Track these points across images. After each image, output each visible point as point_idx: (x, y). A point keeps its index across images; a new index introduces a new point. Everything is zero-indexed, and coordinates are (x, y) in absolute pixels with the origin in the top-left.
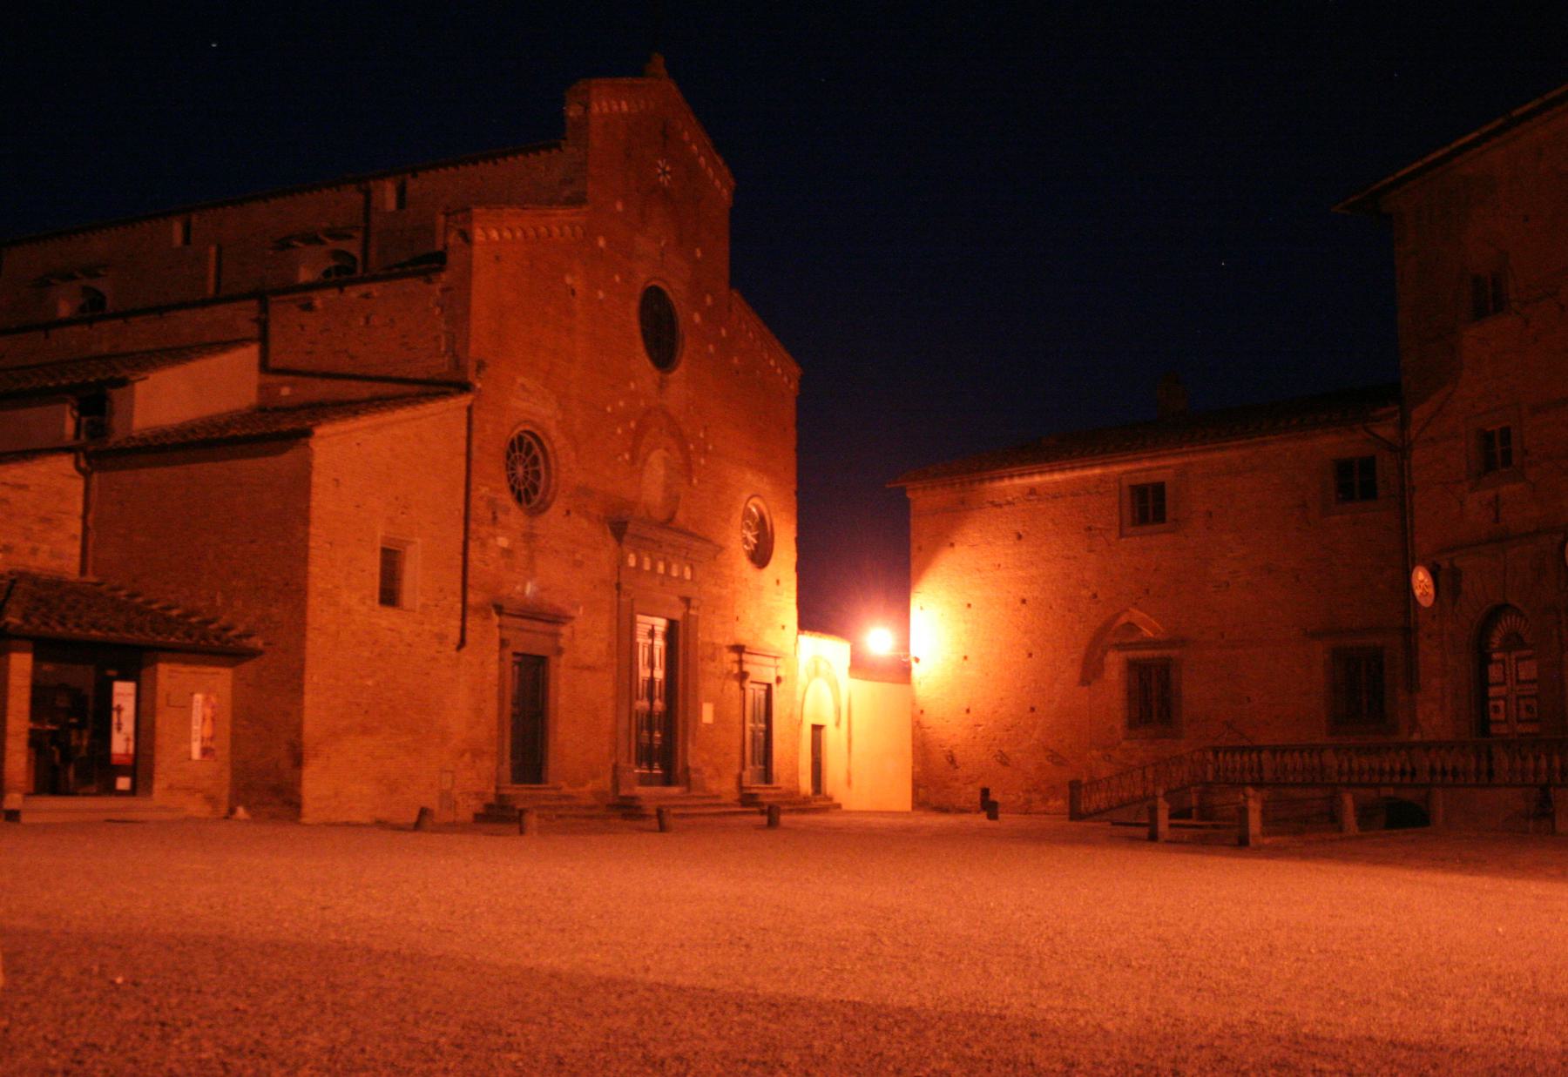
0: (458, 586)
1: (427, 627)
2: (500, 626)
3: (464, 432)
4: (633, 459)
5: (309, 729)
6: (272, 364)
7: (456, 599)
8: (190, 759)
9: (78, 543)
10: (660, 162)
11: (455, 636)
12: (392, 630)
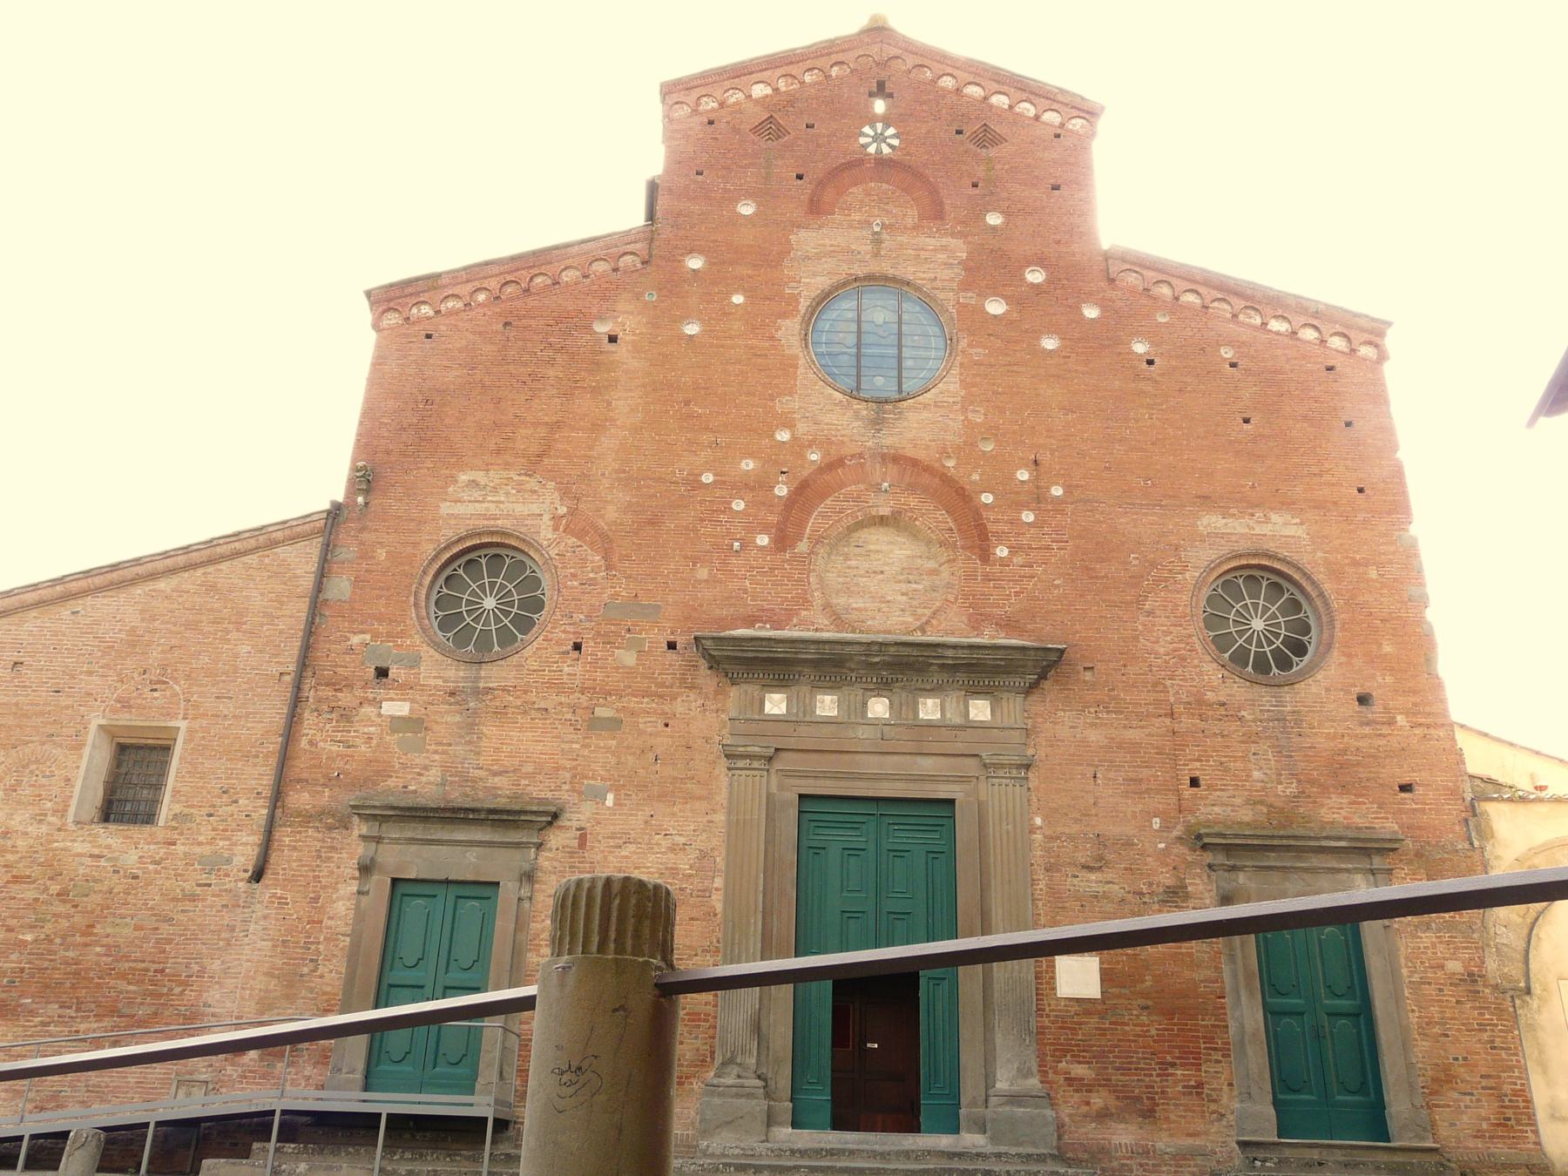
1: (180, 848)
3: (313, 567)
4: (782, 541)
11: (245, 853)
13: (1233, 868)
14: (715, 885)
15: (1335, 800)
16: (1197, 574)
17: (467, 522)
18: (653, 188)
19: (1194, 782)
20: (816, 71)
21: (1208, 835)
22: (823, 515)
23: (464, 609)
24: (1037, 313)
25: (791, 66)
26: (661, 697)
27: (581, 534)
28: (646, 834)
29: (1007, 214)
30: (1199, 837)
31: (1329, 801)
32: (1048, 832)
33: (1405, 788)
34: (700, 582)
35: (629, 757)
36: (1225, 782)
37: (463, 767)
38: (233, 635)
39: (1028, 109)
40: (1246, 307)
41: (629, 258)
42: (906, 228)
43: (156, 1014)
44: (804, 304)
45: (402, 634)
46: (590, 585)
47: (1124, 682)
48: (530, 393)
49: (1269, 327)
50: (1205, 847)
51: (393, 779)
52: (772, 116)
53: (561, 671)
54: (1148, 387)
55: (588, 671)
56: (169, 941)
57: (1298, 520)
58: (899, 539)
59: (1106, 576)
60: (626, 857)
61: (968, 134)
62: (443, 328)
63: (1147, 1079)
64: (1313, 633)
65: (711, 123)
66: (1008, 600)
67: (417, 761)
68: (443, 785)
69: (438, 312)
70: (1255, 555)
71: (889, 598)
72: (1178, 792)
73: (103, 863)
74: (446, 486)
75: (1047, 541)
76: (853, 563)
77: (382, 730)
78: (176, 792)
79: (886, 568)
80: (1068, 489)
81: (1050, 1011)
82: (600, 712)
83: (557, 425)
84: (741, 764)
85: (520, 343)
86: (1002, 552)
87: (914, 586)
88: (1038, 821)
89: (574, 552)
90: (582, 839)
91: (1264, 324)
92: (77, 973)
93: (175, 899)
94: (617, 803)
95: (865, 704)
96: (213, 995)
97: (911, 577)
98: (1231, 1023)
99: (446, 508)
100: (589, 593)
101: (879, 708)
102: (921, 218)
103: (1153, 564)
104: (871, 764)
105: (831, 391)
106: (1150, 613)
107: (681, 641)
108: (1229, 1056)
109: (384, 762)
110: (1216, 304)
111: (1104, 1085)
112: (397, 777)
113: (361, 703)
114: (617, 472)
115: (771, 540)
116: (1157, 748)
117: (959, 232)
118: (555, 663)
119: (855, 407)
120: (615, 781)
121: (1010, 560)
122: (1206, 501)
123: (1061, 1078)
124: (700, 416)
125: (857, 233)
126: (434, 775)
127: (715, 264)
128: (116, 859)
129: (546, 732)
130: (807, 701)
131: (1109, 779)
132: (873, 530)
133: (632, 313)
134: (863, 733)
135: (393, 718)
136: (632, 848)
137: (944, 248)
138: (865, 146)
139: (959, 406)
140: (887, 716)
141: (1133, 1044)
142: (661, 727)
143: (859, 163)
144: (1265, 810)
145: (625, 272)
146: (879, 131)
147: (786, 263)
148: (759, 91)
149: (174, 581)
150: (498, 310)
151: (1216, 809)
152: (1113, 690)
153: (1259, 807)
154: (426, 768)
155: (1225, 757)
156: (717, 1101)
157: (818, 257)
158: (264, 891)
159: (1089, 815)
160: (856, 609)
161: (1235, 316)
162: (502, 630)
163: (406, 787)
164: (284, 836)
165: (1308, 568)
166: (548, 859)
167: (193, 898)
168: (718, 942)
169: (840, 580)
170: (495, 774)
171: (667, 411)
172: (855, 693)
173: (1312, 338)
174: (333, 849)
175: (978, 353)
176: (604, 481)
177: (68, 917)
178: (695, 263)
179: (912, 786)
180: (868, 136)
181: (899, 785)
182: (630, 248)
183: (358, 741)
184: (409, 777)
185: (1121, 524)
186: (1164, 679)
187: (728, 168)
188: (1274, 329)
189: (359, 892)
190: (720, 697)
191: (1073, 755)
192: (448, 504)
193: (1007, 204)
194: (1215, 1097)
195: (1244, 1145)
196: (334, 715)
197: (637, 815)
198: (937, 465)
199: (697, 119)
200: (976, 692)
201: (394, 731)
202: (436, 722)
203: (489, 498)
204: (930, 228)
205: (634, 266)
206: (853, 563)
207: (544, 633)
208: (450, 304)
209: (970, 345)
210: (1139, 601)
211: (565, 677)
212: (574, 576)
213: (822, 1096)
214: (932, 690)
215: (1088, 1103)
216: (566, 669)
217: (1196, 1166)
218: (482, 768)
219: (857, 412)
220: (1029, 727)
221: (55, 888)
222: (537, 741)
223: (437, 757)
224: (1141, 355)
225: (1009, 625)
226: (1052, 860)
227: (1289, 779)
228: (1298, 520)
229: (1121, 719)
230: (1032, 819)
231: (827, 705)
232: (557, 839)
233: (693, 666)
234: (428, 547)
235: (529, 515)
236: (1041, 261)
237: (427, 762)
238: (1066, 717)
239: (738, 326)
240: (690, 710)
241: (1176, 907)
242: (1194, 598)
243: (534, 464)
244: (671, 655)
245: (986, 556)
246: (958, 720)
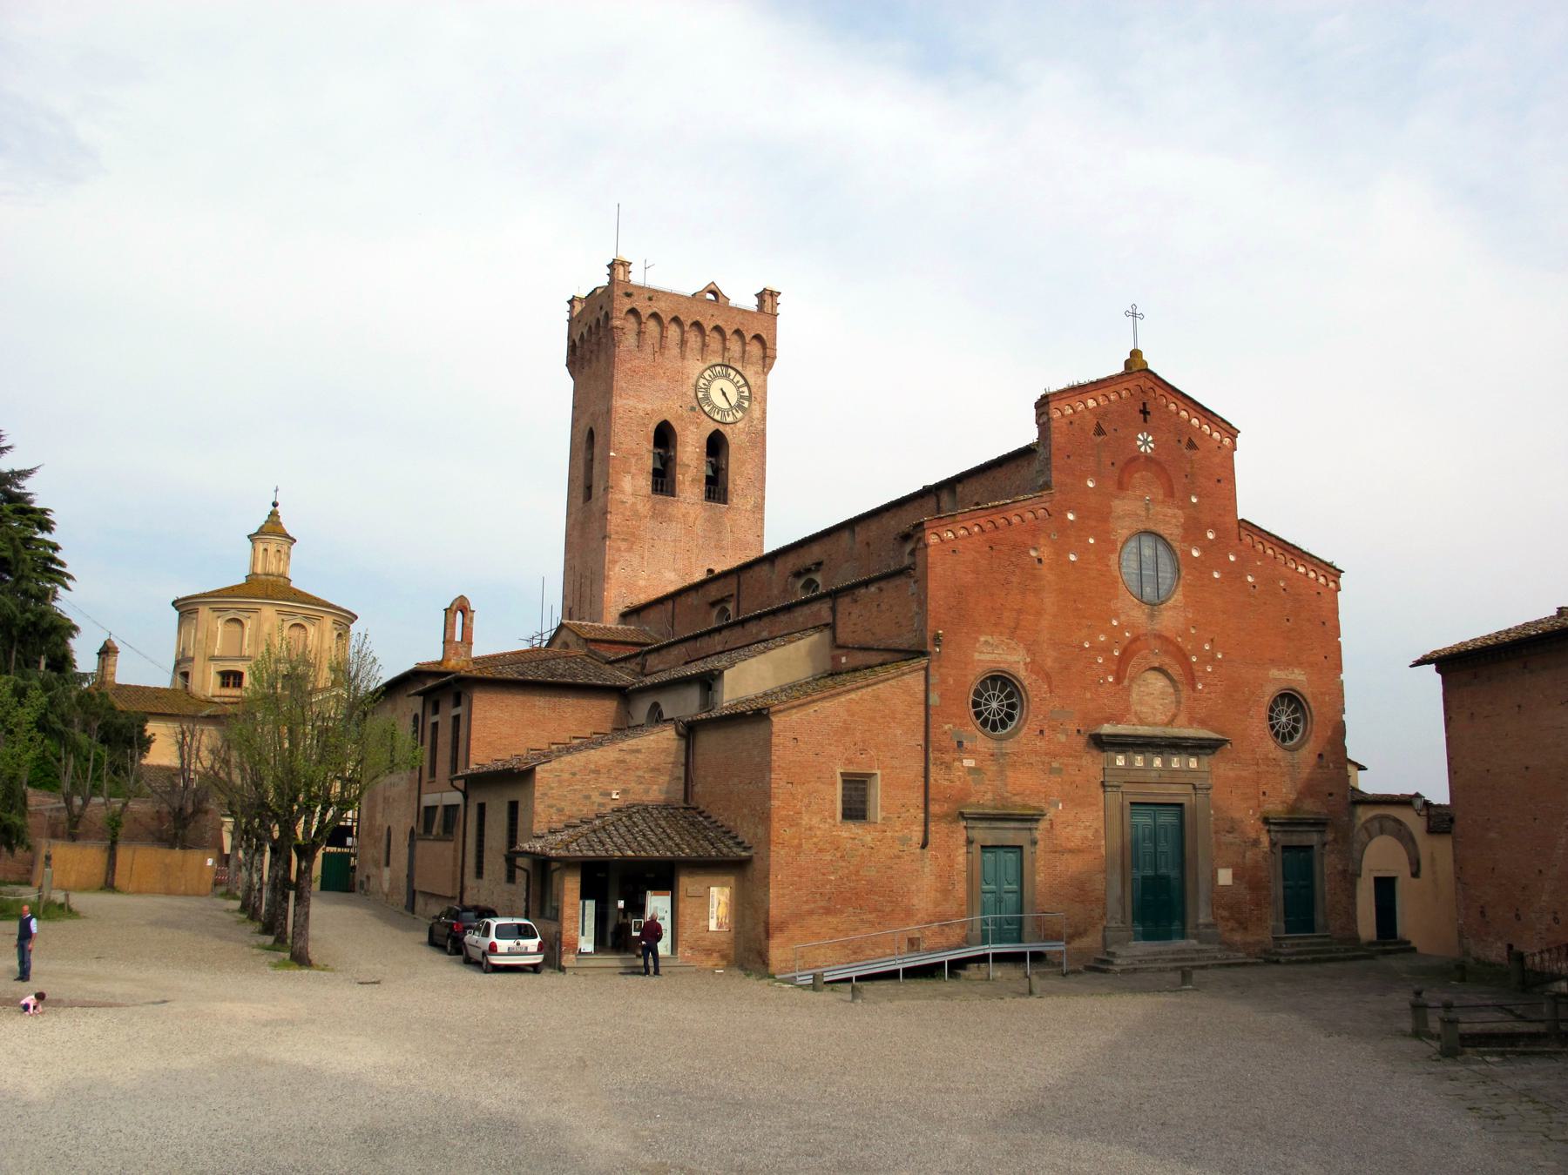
0: (921, 800)
2: (966, 827)
3: (922, 688)
4: (1118, 680)
5: (774, 911)
6: (840, 641)
7: (919, 811)
8: (708, 931)
9: (683, 781)
10: (1140, 436)
11: (917, 836)
12: (854, 839)
19: (1264, 793)
22: (1133, 666)
26: (1076, 757)
27: (1037, 674)
33: (1331, 794)
38: (892, 725)
43: (893, 910)
44: (1119, 545)
56: (892, 877)
62: (961, 547)
65: (1071, 423)
69: (956, 538)
72: (1258, 798)
73: (857, 842)
76: (1142, 689)
78: (882, 806)
82: (1055, 765)
83: (1020, 611)
85: (998, 560)
88: (1212, 812)
90: (1052, 825)
91: (1297, 569)
92: (857, 894)
93: (891, 858)
96: (915, 901)
99: (977, 656)
101: (1157, 762)
102: (1165, 496)
103: (1253, 693)
104: (1156, 789)
105: (1132, 598)
106: (1252, 717)
110: (1279, 556)
114: (1050, 639)
122: (1273, 662)
124: (1081, 609)
126: (989, 796)
128: (861, 840)
133: (1046, 546)
134: (1153, 774)
136: (1070, 828)
138: (1140, 447)
139: (1182, 609)
143: (1135, 459)
145: (1042, 520)
148: (1091, 403)
149: (859, 693)
154: (985, 792)
158: (929, 852)
164: (932, 827)
165: (1306, 696)
167: (899, 857)
170: (1015, 795)
172: (1148, 755)
174: (953, 832)
177: (847, 868)
183: (955, 780)
193: (1199, 490)
195: (1276, 939)
196: (943, 767)
199: (1064, 420)
200: (1192, 755)
206: (1142, 689)
209: (1187, 574)
221: (839, 855)
223: (989, 787)
225: (1203, 723)
231: (1139, 761)
232: (1043, 825)
234: (973, 679)
236: (1214, 527)
238: (1222, 765)
239: (1092, 557)
243: (1013, 632)
245: (1194, 688)
246: (1185, 768)
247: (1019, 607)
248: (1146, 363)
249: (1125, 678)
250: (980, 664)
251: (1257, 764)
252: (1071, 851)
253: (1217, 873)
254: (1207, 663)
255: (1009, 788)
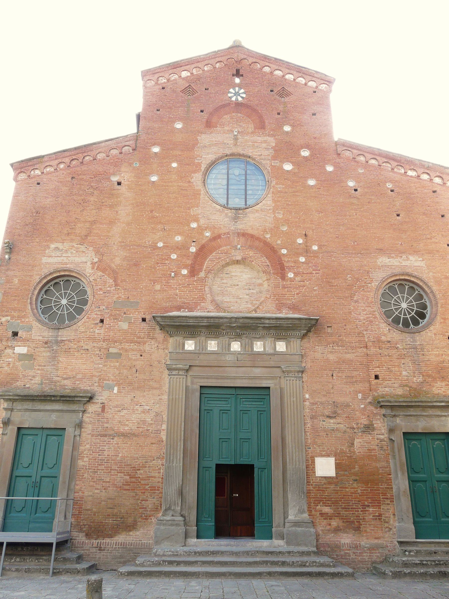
4: (193, 272)
13: (395, 416)
14: (163, 428)
15: (439, 384)
16: (377, 284)
17: (54, 266)
18: (139, 117)
19: (377, 377)
20: (210, 65)
21: (383, 401)
22: (212, 260)
23: (53, 304)
24: (306, 169)
25: (199, 64)
26: (139, 343)
27: (104, 270)
28: (132, 405)
29: (293, 126)
30: (379, 402)
31: (436, 384)
32: (312, 401)
34: (157, 291)
35: (125, 371)
36: (390, 377)
37: (50, 376)
39: (301, 80)
40: (397, 165)
41: (126, 148)
42: (248, 133)
44: (203, 167)
45: (24, 317)
46: (108, 293)
47: (345, 333)
48: (82, 208)
49: (407, 174)
50: (381, 407)
51: (19, 382)
52: (190, 85)
53: (94, 332)
54: (355, 201)
55: (106, 332)
57: (421, 259)
58: (245, 270)
59: (337, 285)
60: (123, 416)
61: (276, 92)
63: (357, 513)
64: (429, 309)
65: (163, 88)
66: (293, 297)
67: (30, 374)
68: (42, 384)
69: (43, 173)
70: (403, 275)
71: (241, 297)
72: (369, 382)
74: (45, 250)
75: (311, 270)
76: (225, 281)
77: (15, 360)
79: (239, 283)
80: (320, 247)
81: (313, 482)
82: (112, 350)
83: (93, 223)
84: (174, 373)
85: (79, 186)
86: (291, 275)
87: (252, 291)
88: (307, 396)
89: (101, 278)
94: (119, 391)
95: (229, 345)
97: (251, 287)
98: (394, 486)
99: (45, 260)
100: (108, 297)
101: (236, 346)
102: (255, 128)
103: (358, 280)
104: (232, 372)
105: (215, 205)
106: (356, 301)
107: (148, 317)
108: (393, 501)
109: (16, 374)
110: (384, 164)
111: (337, 516)
112: (21, 381)
113: (5, 348)
114: (120, 242)
115: (188, 272)
116: (360, 362)
117: (272, 134)
118: (92, 328)
119: (226, 212)
120: (118, 381)
121: (294, 278)
122: (381, 251)
123: (318, 513)
124: (157, 217)
125: (227, 135)
126: (37, 380)
127: (164, 150)
129: (88, 360)
130: (204, 344)
131: (339, 377)
132: (234, 266)
133: (128, 172)
134: (229, 358)
135: (19, 354)
136: (125, 411)
137: (265, 142)
138: (230, 98)
140: (240, 350)
141: (350, 497)
142: (139, 356)
144: (408, 389)
145: (125, 154)
146: (237, 91)
147: (196, 149)
148: (185, 74)
150: (69, 172)
151: (386, 389)
152: (340, 336)
153: (405, 388)
154: (34, 377)
155: (390, 365)
156: (162, 527)
157: (210, 146)
159: (330, 393)
160: (226, 302)
161: (393, 169)
162: (70, 314)
163: (25, 385)
166: (88, 417)
168: (164, 454)
169: (219, 289)
171: (143, 215)
172: (225, 340)
173: (426, 178)
175: (280, 187)
176: (114, 246)
178: (156, 149)
179: (251, 381)
180: (232, 93)
181: (244, 381)
182: (127, 143)
183: (4, 365)
184: (26, 381)
185: (344, 261)
186: (363, 331)
187: (170, 108)
188: (410, 175)
189: (3, 434)
190: (165, 342)
191: (323, 366)
192: (46, 258)
193: (292, 121)
194: (387, 521)
197: (127, 397)
198: (262, 237)
199: (157, 87)
200: (279, 339)
201: (20, 360)
202: (39, 356)
203: (64, 255)
204: (259, 133)
205: (129, 151)
206: (225, 281)
207: (87, 315)
208: (48, 169)
209: (277, 184)
210: (352, 297)
211: (96, 335)
212: (101, 289)
213: (211, 523)
214: (259, 338)
215: (330, 525)
216: (97, 331)
217: (379, 553)
218: (59, 376)
219: (226, 214)
220: (303, 354)
222: (83, 364)
223: (39, 372)
224: (352, 187)
226: (313, 414)
227: (419, 375)
228: (421, 259)
229: (344, 349)
230: (304, 395)
232: (92, 408)
233: (153, 329)
235: (81, 262)
236: (307, 147)
237: (34, 374)
238: (319, 349)
239: (174, 177)
240: (152, 348)
241: (369, 434)
242: (376, 295)
243: (83, 239)
244: (144, 324)
245: (283, 277)
246: (271, 351)
247: (93, 219)
248: (241, 42)
249: (201, 270)
250: (47, 266)
251: (366, 347)
252: (124, 435)
253: (313, 462)
254: (299, 255)
255: (59, 373)
